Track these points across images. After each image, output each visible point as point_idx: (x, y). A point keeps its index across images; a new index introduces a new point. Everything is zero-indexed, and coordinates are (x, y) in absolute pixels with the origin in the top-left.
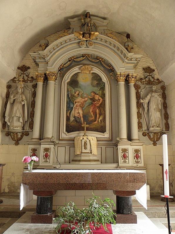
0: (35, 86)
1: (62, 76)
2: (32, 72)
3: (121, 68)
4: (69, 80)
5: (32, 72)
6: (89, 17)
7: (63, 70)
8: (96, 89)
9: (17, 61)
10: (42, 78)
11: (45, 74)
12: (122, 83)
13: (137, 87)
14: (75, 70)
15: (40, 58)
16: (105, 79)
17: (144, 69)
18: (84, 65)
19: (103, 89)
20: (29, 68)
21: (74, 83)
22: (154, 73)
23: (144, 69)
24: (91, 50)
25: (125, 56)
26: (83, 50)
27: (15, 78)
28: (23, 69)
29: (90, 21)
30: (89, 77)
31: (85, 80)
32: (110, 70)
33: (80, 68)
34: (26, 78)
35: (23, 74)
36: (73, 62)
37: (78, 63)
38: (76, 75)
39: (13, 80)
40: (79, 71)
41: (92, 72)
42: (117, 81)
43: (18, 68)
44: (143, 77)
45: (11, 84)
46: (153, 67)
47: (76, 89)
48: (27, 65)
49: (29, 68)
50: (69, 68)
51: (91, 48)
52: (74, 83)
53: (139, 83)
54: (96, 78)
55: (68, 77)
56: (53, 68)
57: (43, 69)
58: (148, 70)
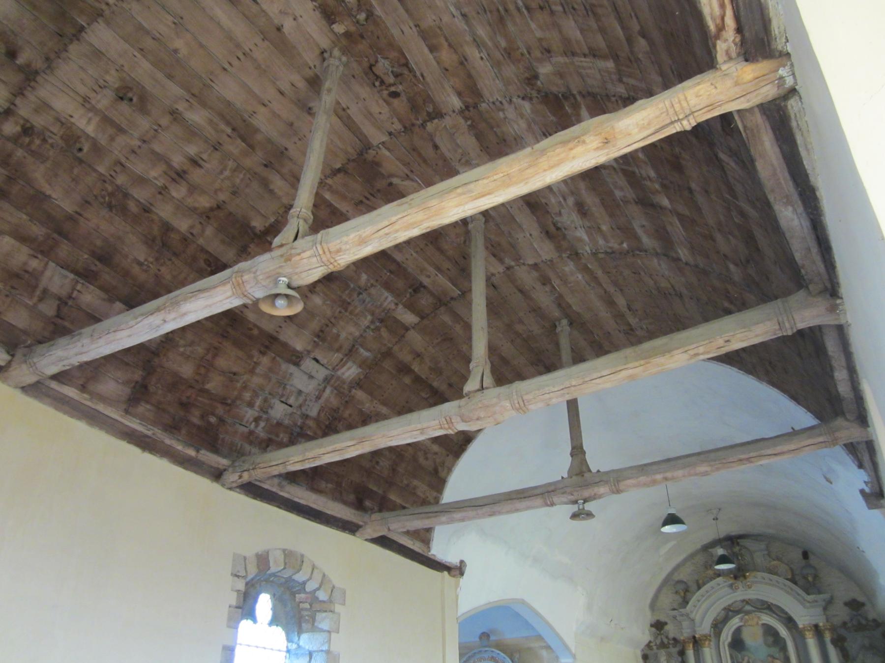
0: (682, 653)
1: (718, 634)
2: (671, 630)
3: (804, 616)
4: (729, 639)
5: (671, 630)
6: (738, 544)
7: (718, 626)
8: (775, 651)
9: (649, 617)
10: (691, 645)
11: (694, 637)
12: (811, 642)
13: (839, 642)
14: (735, 622)
15: (682, 615)
16: (783, 632)
17: (846, 604)
18: (747, 613)
19: (784, 649)
20: (666, 623)
21: (737, 644)
22: (866, 608)
23: (846, 604)
24: (752, 594)
25: (805, 600)
26: (741, 594)
27: (650, 642)
28: (658, 626)
29: (740, 550)
30: (759, 631)
31: (753, 638)
32: (789, 622)
33: (741, 619)
34: (666, 641)
35: (661, 634)
36: (729, 612)
37: (738, 612)
38: (738, 630)
39: (649, 646)
40: (741, 624)
41: (760, 622)
42: (803, 638)
43: (652, 626)
44: (847, 619)
45: (648, 652)
46: (861, 599)
47: (743, 653)
48: (663, 619)
49: (666, 623)
50: (726, 620)
51: (750, 591)
52: (737, 644)
53: (843, 632)
54: (770, 631)
55: (727, 636)
56: (704, 628)
57: (689, 631)
58: (854, 605)
